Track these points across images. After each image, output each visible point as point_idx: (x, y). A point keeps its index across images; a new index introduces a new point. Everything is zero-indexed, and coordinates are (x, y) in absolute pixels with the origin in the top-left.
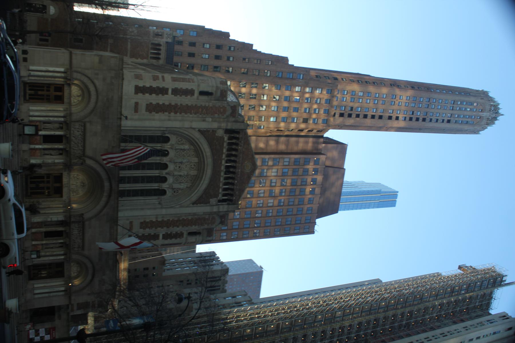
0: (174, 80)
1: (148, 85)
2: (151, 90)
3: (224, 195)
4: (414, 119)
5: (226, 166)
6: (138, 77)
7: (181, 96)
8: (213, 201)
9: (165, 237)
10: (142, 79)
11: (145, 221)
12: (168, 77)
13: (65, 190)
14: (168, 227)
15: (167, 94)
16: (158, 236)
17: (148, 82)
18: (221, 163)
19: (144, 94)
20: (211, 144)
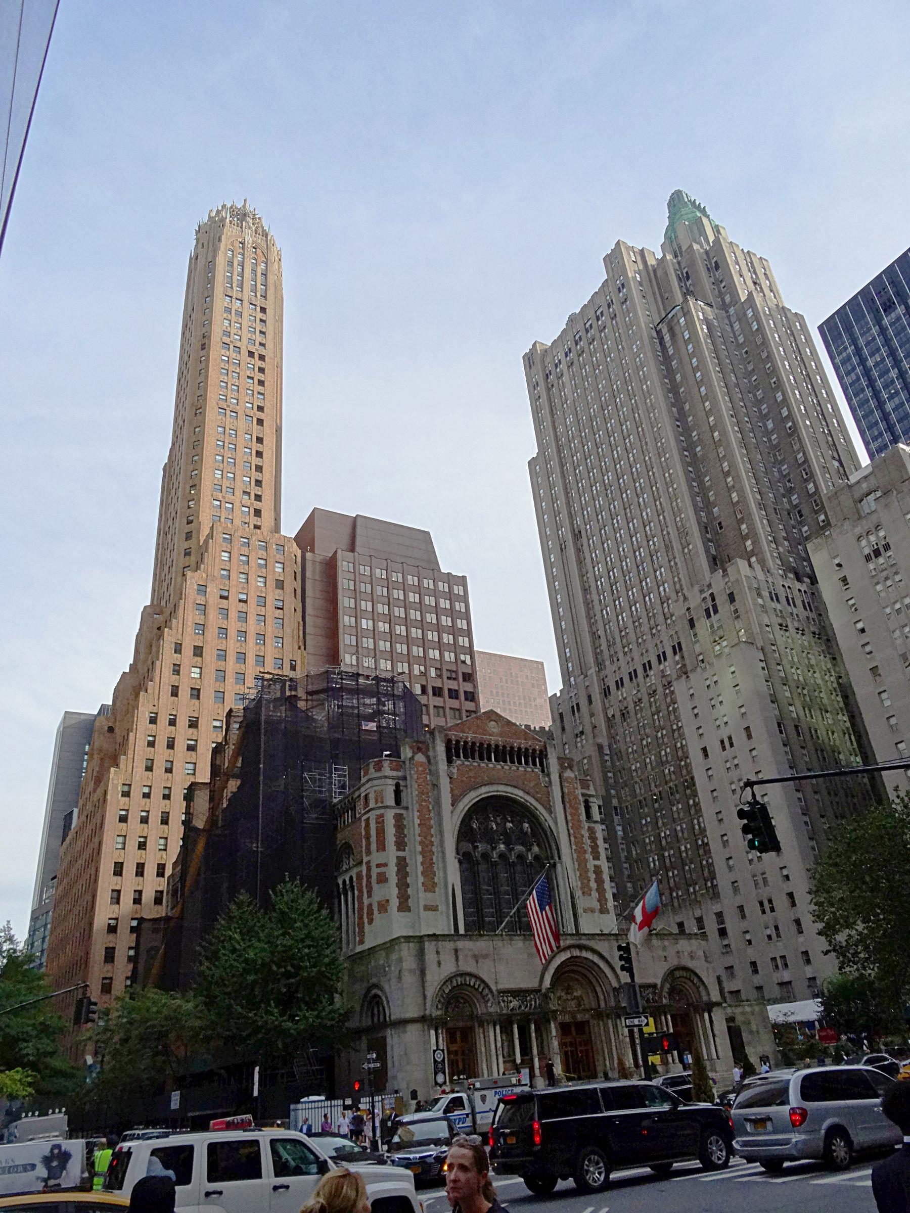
0: (382, 847)
1: (395, 891)
2: (403, 885)
3: (534, 764)
4: (261, 377)
6: (383, 906)
7: (406, 836)
8: (543, 780)
9: (597, 857)
10: (388, 901)
11: (581, 889)
12: (376, 857)
13: (579, 1017)
14: (585, 852)
15: (405, 858)
16: (595, 866)
18: (493, 769)
19: (409, 897)
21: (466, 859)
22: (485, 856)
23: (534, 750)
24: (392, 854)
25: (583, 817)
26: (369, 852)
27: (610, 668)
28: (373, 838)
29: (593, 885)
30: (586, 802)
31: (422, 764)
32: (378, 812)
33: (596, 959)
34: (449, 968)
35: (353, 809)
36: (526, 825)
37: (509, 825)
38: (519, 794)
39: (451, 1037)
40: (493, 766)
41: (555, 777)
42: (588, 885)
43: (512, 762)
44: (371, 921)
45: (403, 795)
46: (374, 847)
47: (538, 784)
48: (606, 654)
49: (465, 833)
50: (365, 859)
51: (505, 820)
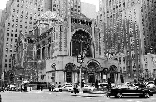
0: (57, 38)
2: (61, 46)
3: (89, 25)
5: (81, 23)
6: (56, 50)
8: (91, 28)
12: (56, 41)
17: (58, 47)
20: (75, 28)
21: (73, 42)
22: (77, 42)
23: (89, 22)
24: (58, 40)
25: (98, 36)
26: (54, 39)
27: (109, 7)
28: (55, 37)
29: (98, 49)
30: (99, 33)
31: (66, 23)
32: (56, 32)
33: (96, 62)
34: (68, 62)
35: (52, 31)
36: (86, 37)
37: (83, 36)
38: (85, 31)
39: (68, 74)
40: (81, 25)
41: (93, 28)
42: (97, 49)
43: (85, 24)
44: (54, 52)
45: (62, 29)
46: (55, 38)
47: (90, 29)
48: (109, 4)
49: (74, 37)
50: (53, 41)
51: (82, 35)
